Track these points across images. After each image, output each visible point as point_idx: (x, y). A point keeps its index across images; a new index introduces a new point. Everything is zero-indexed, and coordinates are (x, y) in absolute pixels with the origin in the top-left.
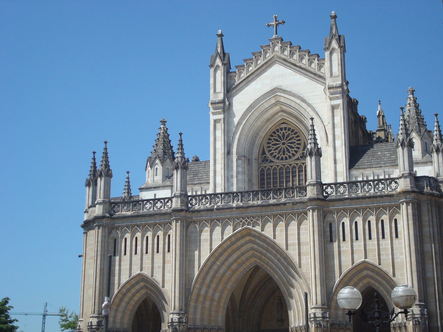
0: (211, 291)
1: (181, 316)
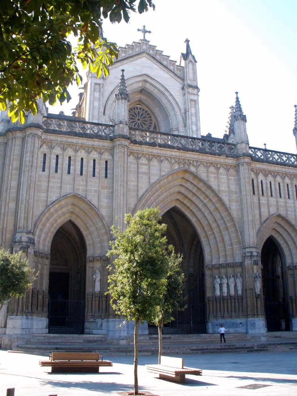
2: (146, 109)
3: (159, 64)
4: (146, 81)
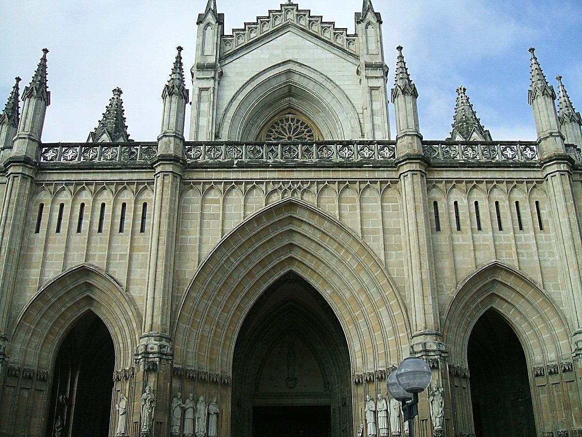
1: (164, 342)
2: (304, 119)
3: (314, 40)
4: (289, 71)
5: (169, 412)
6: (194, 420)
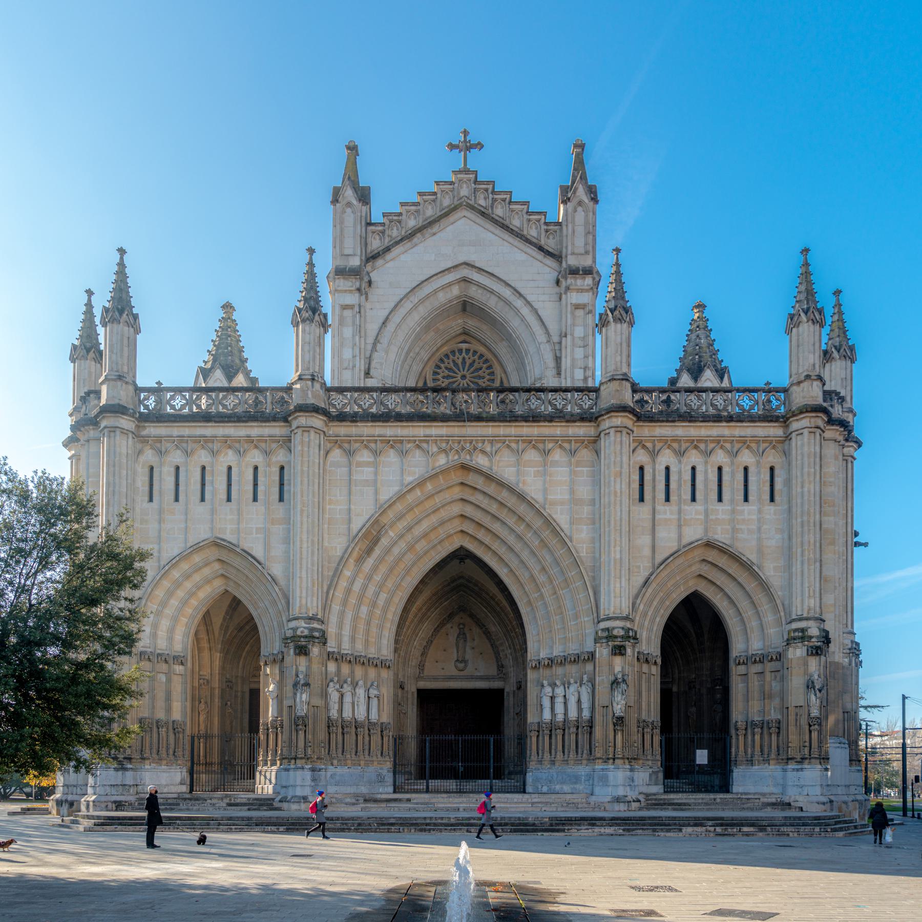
0: (371, 589)
3: (498, 231)
4: (465, 280)
5: (325, 695)
6: (353, 704)
